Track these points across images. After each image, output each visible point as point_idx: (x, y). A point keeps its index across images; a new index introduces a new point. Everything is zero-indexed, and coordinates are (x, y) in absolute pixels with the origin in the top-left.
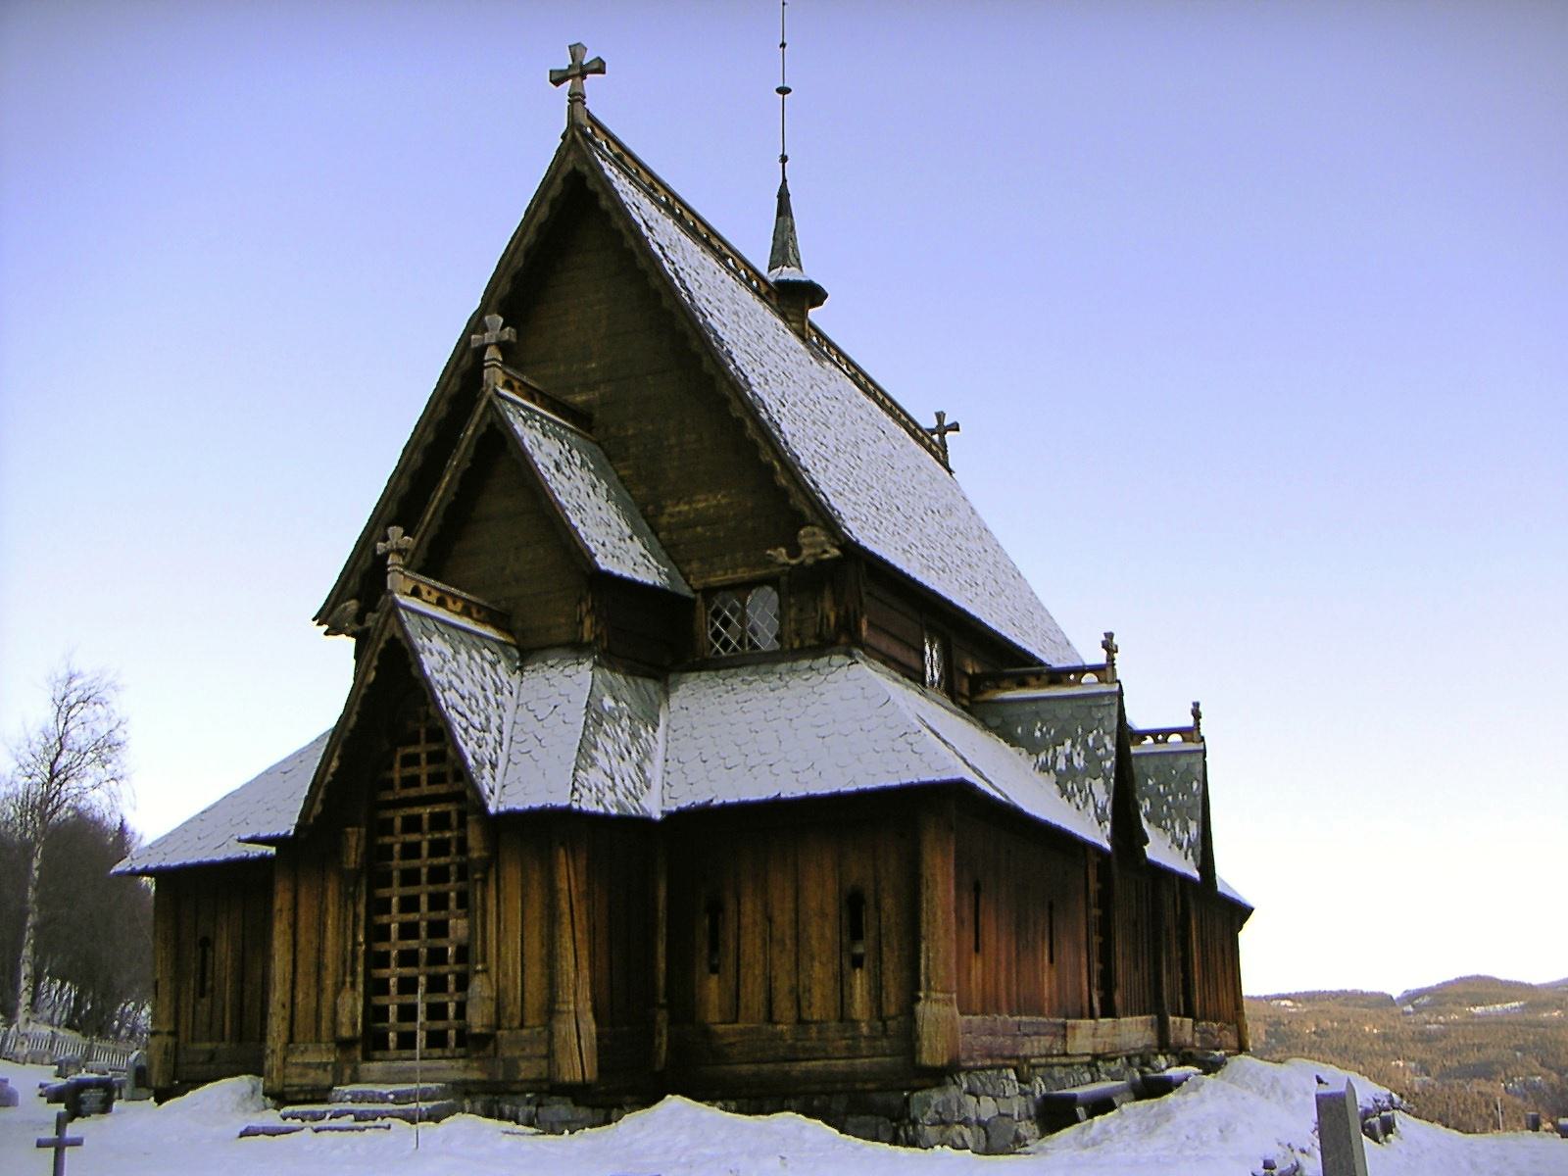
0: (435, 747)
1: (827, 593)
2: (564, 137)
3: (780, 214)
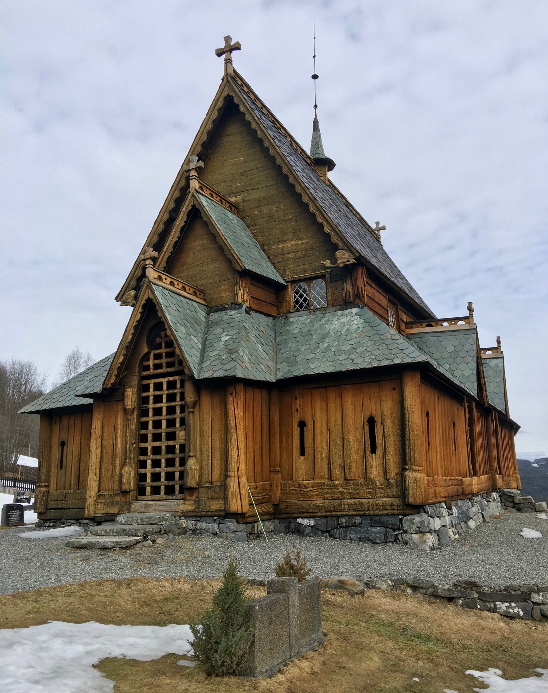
0: (169, 350)
1: (349, 282)
2: (223, 80)
3: (314, 130)
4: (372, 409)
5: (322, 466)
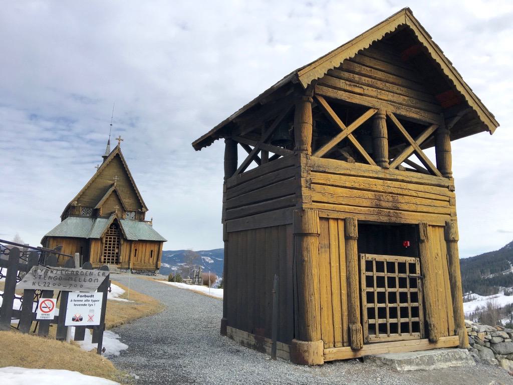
4: (152, 248)
5: (139, 259)
